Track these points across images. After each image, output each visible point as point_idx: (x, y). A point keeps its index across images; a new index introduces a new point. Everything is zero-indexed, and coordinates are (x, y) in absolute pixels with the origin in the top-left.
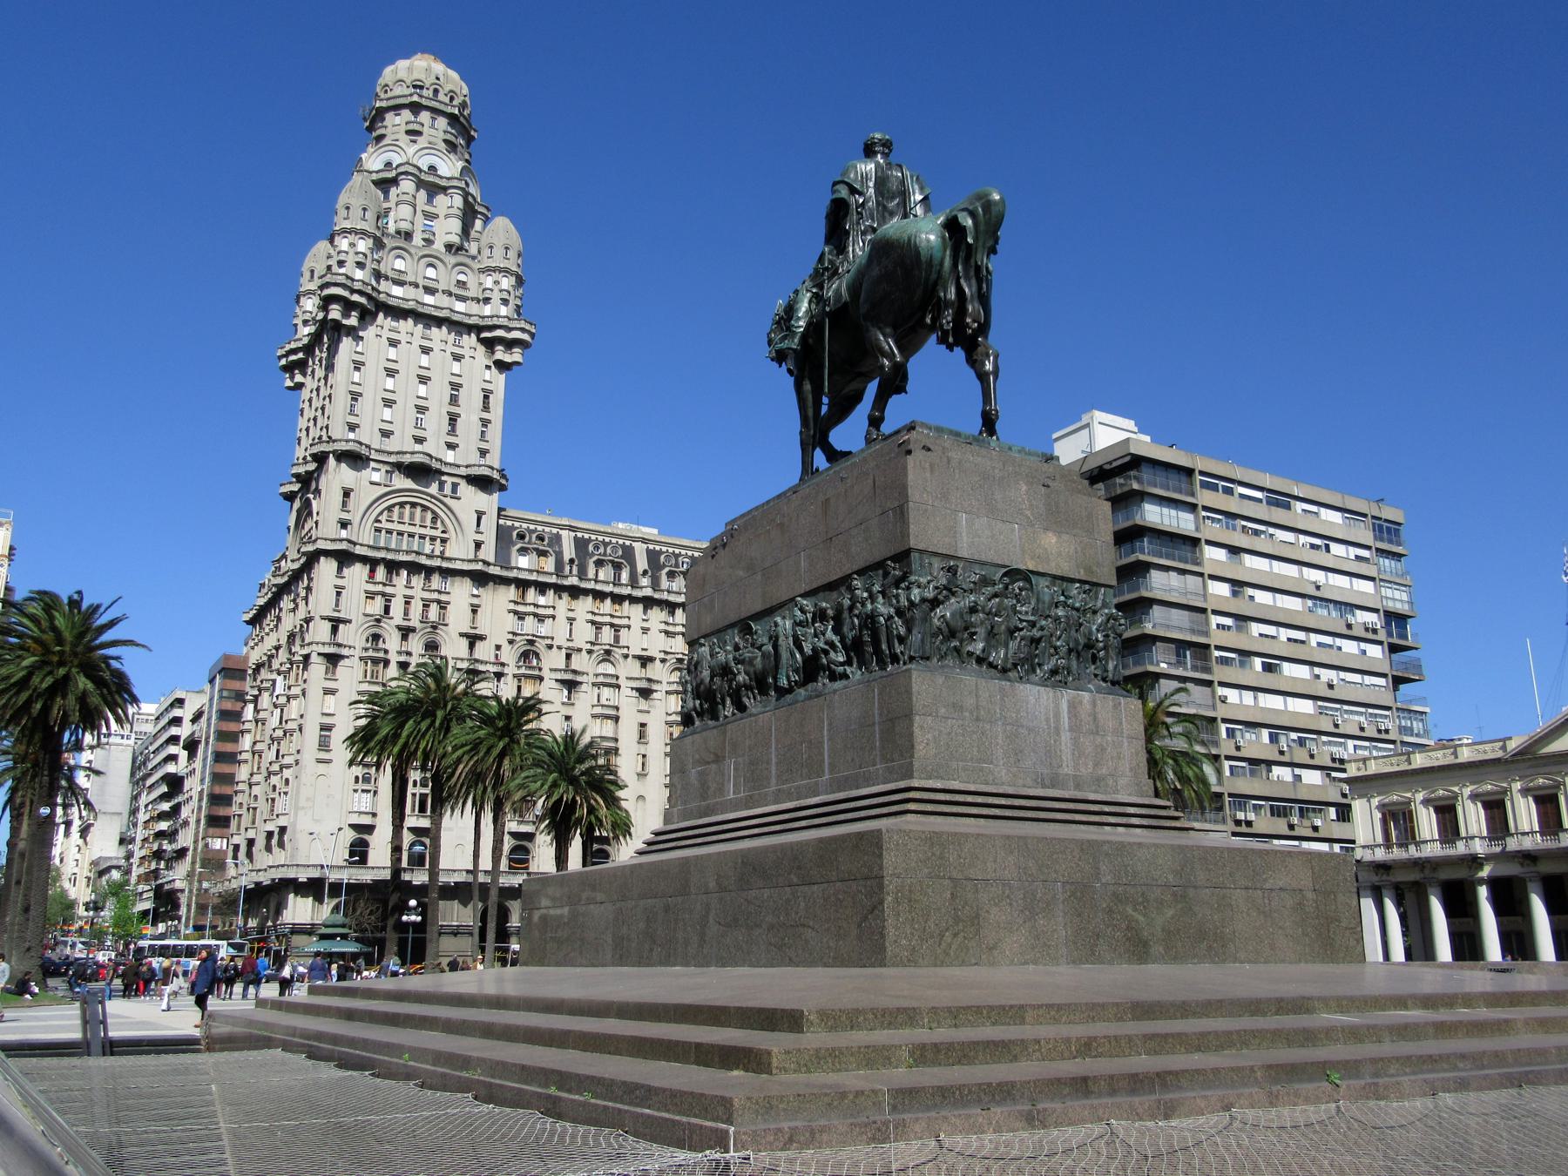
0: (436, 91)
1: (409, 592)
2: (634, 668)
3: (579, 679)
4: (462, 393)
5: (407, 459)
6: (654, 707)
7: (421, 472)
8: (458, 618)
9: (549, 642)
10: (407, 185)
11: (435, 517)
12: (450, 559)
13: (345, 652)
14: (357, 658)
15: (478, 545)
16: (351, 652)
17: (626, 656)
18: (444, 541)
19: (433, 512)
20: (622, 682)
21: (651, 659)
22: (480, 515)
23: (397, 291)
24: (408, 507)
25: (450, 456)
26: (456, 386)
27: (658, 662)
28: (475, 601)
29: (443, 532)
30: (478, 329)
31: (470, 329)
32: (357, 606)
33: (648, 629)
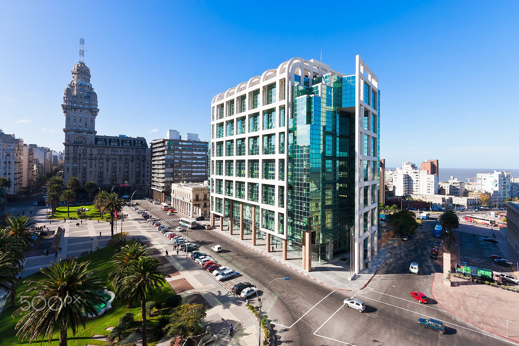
2: (119, 157)
11: (84, 138)
15: (91, 142)
20: (117, 159)
21: (122, 155)
25: (86, 129)
30: (90, 110)
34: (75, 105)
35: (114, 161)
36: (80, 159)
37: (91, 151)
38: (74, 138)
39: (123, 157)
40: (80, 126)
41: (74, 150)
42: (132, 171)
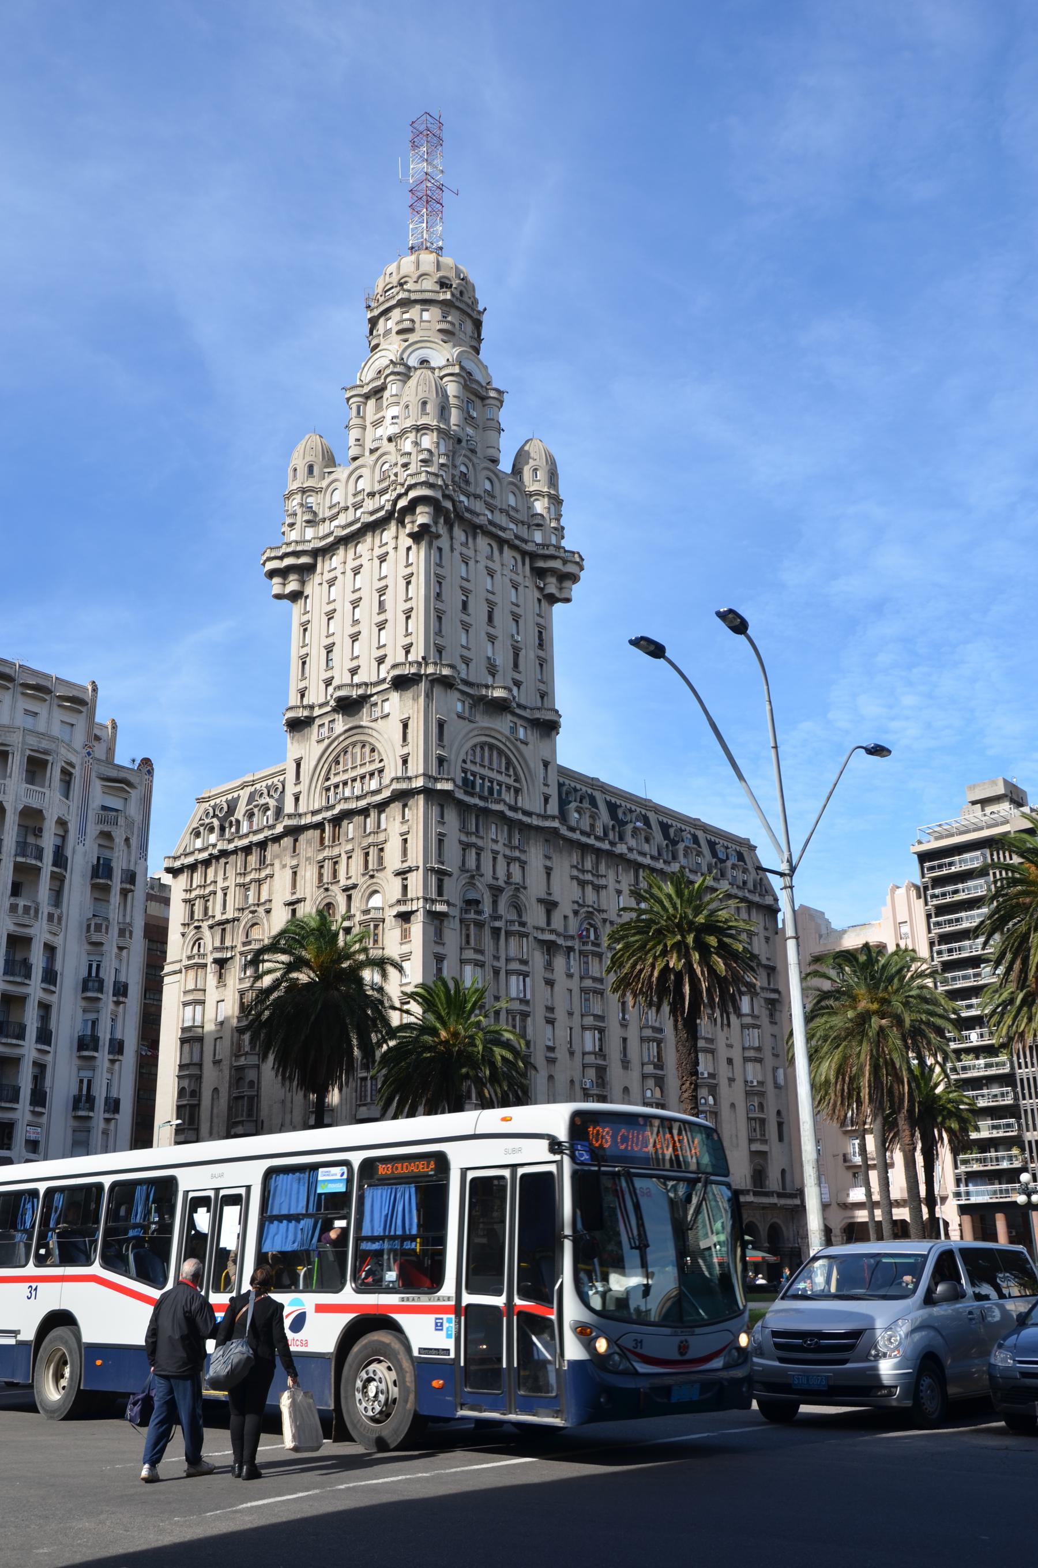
0: (461, 293)
1: (495, 847)
9: (605, 916)
11: (509, 763)
14: (457, 920)
15: (546, 800)
18: (517, 791)
19: (508, 759)
24: (486, 749)
28: (548, 863)
29: (515, 781)
30: (533, 556)
31: (524, 553)
37: (548, 871)
38: (462, 756)
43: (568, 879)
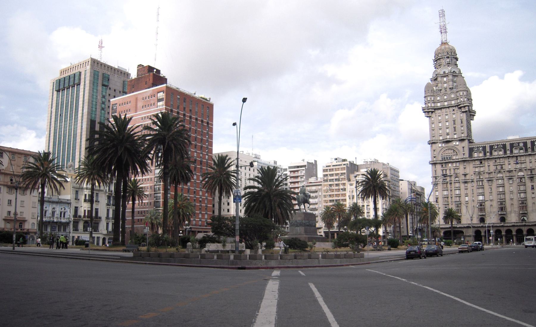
1: (450, 168)
3: (493, 179)
4: (456, 121)
5: (445, 140)
6: (514, 182)
7: (448, 142)
8: (461, 171)
9: (484, 172)
10: (439, 79)
11: (454, 150)
12: (458, 159)
13: (438, 183)
14: (441, 184)
15: (464, 154)
16: (440, 182)
17: (505, 171)
19: (454, 150)
20: (504, 178)
22: (463, 147)
23: (439, 104)
25: (455, 136)
26: (454, 121)
27: (514, 171)
28: (465, 167)
30: (458, 106)
31: (455, 106)
32: (439, 173)
33: (510, 164)
34: (439, 104)
35: (500, 182)
36: (451, 183)
39: (514, 173)
40: (448, 134)
41: (443, 170)
42: (533, 198)
43: (472, 168)
